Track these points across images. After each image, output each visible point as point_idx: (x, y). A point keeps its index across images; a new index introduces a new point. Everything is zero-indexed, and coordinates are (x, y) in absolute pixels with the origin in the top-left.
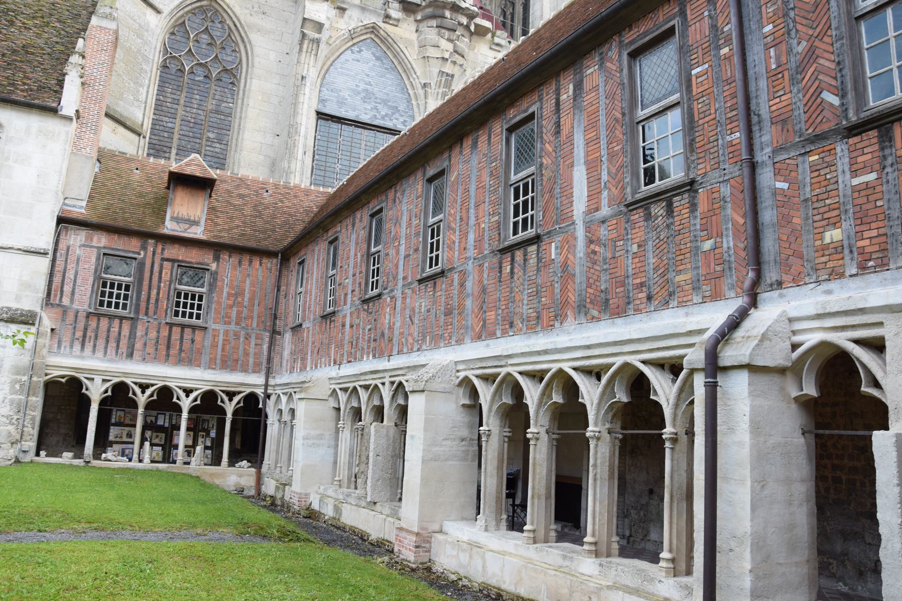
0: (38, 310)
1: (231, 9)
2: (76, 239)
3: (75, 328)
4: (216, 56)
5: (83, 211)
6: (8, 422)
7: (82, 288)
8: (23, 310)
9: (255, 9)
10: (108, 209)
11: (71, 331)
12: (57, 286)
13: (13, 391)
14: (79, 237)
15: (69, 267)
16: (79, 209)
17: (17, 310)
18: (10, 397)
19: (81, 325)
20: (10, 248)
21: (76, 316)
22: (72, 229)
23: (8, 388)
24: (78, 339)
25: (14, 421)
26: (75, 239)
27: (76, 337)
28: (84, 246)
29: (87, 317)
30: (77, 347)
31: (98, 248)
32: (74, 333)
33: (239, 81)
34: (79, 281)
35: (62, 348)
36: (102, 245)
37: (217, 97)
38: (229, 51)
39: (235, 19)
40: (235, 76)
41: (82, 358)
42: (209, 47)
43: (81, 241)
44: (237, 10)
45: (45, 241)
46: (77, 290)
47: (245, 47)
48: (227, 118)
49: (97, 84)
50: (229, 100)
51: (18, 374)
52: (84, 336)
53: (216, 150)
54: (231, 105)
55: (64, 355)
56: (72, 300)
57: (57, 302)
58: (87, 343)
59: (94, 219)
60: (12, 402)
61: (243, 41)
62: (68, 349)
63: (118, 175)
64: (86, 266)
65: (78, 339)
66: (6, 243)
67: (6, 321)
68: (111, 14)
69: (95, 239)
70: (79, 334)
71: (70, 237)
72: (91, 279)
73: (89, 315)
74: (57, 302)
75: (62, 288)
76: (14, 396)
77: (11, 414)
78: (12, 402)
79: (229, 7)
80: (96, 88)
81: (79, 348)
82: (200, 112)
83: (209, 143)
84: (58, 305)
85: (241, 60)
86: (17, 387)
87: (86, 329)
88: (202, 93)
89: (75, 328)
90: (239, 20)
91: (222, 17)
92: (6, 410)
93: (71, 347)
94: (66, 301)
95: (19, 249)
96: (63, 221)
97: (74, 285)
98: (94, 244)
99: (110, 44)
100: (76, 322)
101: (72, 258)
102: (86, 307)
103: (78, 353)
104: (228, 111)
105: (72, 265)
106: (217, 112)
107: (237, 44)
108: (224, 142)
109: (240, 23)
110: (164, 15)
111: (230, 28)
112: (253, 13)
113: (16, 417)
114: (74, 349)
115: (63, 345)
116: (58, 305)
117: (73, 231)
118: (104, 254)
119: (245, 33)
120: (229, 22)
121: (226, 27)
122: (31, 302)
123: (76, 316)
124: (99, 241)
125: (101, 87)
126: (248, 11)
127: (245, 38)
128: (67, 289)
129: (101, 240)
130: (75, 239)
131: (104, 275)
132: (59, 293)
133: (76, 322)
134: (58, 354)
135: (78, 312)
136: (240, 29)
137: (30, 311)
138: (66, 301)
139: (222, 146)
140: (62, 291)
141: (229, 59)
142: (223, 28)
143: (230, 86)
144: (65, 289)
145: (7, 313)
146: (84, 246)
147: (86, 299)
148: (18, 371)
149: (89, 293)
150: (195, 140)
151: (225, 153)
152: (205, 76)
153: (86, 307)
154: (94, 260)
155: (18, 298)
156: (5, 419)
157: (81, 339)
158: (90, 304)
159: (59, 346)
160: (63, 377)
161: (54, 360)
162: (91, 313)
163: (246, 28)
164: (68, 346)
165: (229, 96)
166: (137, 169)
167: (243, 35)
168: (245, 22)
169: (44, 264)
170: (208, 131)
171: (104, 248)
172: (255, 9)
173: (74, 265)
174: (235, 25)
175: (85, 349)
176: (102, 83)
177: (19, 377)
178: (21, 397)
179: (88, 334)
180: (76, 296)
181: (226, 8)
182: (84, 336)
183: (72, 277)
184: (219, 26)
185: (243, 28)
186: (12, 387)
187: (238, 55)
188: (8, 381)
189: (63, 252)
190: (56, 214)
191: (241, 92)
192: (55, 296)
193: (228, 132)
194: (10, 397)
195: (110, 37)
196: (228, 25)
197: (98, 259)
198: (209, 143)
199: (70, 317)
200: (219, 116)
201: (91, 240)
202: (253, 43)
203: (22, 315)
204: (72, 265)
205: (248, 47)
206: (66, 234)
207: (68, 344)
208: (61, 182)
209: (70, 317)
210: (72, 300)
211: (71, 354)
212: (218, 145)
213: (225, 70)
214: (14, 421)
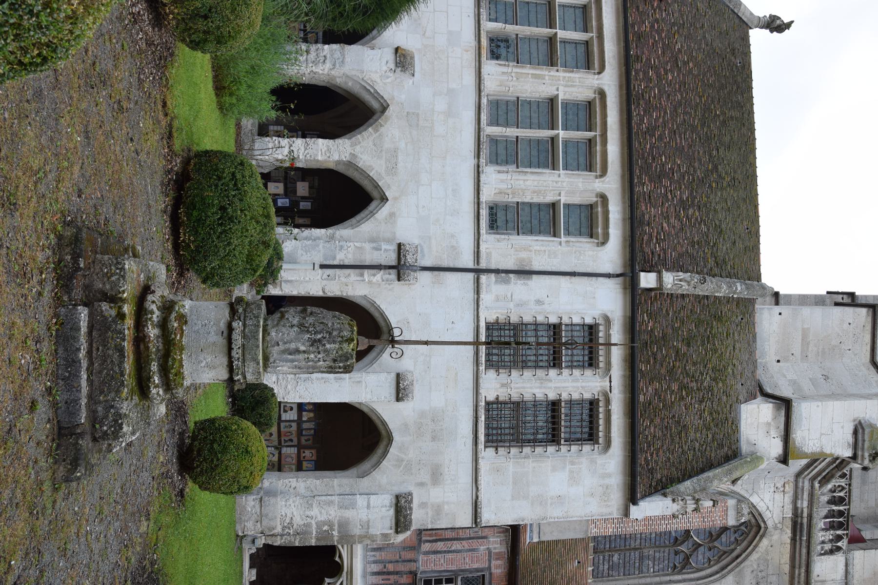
0: (413, 528)
1: (753, 550)
2: (497, 545)
3: (397, 561)
4: (700, 545)
5: (528, 541)
6: (286, 524)
7: (442, 561)
8: (411, 515)
9: (760, 574)
10: (533, 564)
11: (393, 559)
12: (441, 535)
13: (319, 525)
14: (499, 545)
15: (464, 542)
16: (529, 538)
17: (411, 509)
18: (313, 523)
19: (401, 567)
20: (477, 488)
21: (410, 561)
22: (506, 536)
23: (322, 519)
24: (385, 567)
25: (287, 530)
26: (495, 542)
27: (387, 565)
28: (490, 553)
29: (410, 572)
30: (375, 568)
31: (489, 568)
32: (391, 562)
33: (679, 573)
34: (449, 556)
35: (373, 553)
36: (493, 570)
37: (657, 555)
38: (708, 554)
39: (744, 555)
40: (683, 568)
41: (364, 576)
42: (707, 534)
43: (495, 548)
44: (754, 556)
45: (488, 517)
46: (439, 556)
47: (717, 573)
48: (637, 569)
49: (666, 522)
50: (656, 568)
51: (339, 526)
52: (389, 573)
53: (601, 566)
54: (652, 569)
55: (365, 557)
56: (427, 553)
57: (424, 538)
58: (381, 577)
59: (521, 558)
60: (308, 525)
61: (723, 569)
62: (373, 559)
63: (569, 550)
64: (467, 560)
65: (385, 567)
66: (482, 482)
67: (396, 505)
68: (743, 515)
69: (499, 562)
70: (391, 567)
71: (497, 537)
72: (454, 568)
73: (414, 574)
74: (424, 538)
75: (440, 540)
76: (314, 526)
77: (295, 527)
78: (308, 525)
79: (756, 546)
80: (663, 522)
81: (375, 571)
82: (638, 541)
83: (607, 558)
84: (420, 540)
85: (701, 570)
86: (326, 528)
87: (397, 573)
88: (658, 538)
89: (397, 561)
90: (744, 560)
91: (743, 541)
92: (298, 521)
93: (375, 562)
94: (426, 547)
95: (477, 497)
96: (514, 532)
97: (445, 552)
98: (493, 562)
99: (711, 523)
100: (404, 561)
101: (474, 544)
102: (421, 568)
103: (369, 570)
104: (645, 569)
105: (466, 545)
106: (641, 559)
107: (718, 562)
108: (610, 572)
109: (741, 562)
110: (732, 487)
111: (733, 550)
112: (755, 572)
113: (291, 532)
114: (373, 565)
115: (377, 554)
116: (420, 540)
117: (504, 538)
118: (483, 576)
119: (732, 570)
120: (739, 549)
121: (732, 547)
122: (419, 518)
123: (410, 561)
124: (497, 567)
125: (664, 526)
126: (755, 567)
127: (726, 570)
128: (440, 546)
129: (498, 569)
130: (495, 542)
131: (459, 579)
132: (434, 538)
133: (404, 561)
134: (366, 549)
135: (415, 561)
136: (735, 563)
137: (411, 522)
138: (426, 547)
139: (606, 571)
140: (436, 541)
141: (700, 557)
142: (731, 543)
143: (671, 565)
144: (439, 543)
145: (405, 502)
146: (490, 553)
147: (431, 567)
148: (343, 525)
149: (438, 568)
150: (608, 543)
151: (600, 575)
152: (676, 539)
153: (421, 568)
154: (476, 566)
155: (423, 505)
156: (288, 521)
157: (385, 570)
158: (425, 572)
159: (374, 550)
160: (340, 557)
161: (359, 550)
162: (416, 575)
163: (737, 569)
164: (375, 559)
165: (661, 566)
166: (579, 562)
167: (729, 568)
168: (744, 567)
169: (464, 520)
170: (619, 555)
171: (491, 574)
172: (760, 574)
173: (467, 547)
174: (737, 557)
175: (374, 577)
176: (668, 526)
177: (336, 527)
178: (314, 533)
179: (391, 577)
180: (432, 557)
181: (754, 544)
182: (389, 573)
183: (453, 548)
184: (732, 539)
185: (737, 566)
186: (324, 523)
187: (706, 565)
188: (330, 518)
189: (480, 533)
190: (521, 523)
191: (668, 578)
192: (430, 535)
193: (622, 574)
194: (313, 523)
195: (719, 522)
196: (736, 548)
197: (477, 570)
198: (607, 558)
199: (409, 555)
200: (637, 561)
201: (497, 559)
202: (723, 580)
203: (405, 517)
204: (466, 545)
205: (718, 576)
206: (500, 532)
207: (378, 558)
208: (556, 520)
209: (409, 555)
210: (427, 553)
211: (366, 562)
212: (606, 567)
213: (687, 558)
214: (287, 530)
